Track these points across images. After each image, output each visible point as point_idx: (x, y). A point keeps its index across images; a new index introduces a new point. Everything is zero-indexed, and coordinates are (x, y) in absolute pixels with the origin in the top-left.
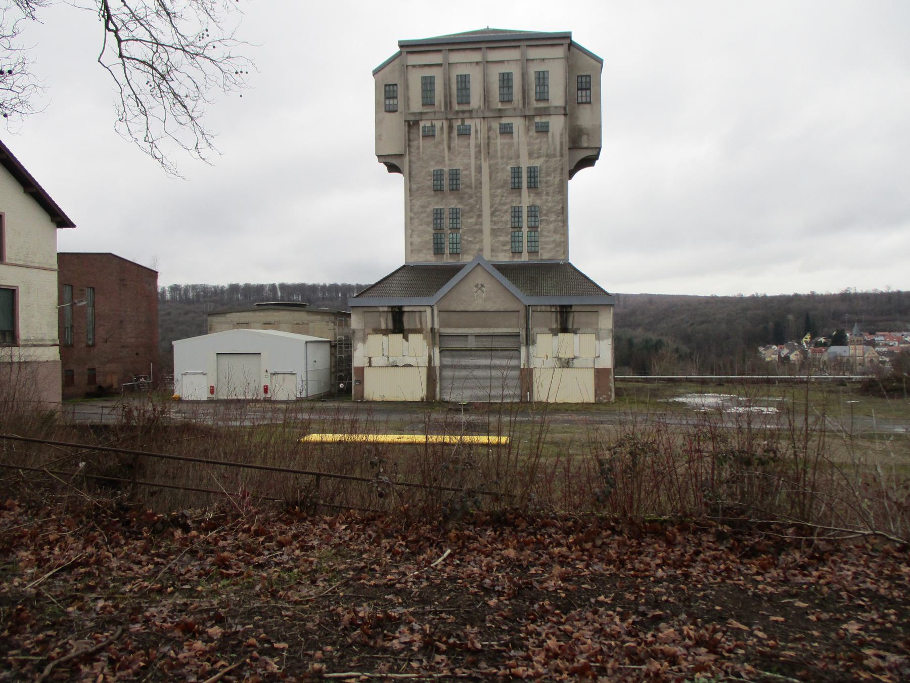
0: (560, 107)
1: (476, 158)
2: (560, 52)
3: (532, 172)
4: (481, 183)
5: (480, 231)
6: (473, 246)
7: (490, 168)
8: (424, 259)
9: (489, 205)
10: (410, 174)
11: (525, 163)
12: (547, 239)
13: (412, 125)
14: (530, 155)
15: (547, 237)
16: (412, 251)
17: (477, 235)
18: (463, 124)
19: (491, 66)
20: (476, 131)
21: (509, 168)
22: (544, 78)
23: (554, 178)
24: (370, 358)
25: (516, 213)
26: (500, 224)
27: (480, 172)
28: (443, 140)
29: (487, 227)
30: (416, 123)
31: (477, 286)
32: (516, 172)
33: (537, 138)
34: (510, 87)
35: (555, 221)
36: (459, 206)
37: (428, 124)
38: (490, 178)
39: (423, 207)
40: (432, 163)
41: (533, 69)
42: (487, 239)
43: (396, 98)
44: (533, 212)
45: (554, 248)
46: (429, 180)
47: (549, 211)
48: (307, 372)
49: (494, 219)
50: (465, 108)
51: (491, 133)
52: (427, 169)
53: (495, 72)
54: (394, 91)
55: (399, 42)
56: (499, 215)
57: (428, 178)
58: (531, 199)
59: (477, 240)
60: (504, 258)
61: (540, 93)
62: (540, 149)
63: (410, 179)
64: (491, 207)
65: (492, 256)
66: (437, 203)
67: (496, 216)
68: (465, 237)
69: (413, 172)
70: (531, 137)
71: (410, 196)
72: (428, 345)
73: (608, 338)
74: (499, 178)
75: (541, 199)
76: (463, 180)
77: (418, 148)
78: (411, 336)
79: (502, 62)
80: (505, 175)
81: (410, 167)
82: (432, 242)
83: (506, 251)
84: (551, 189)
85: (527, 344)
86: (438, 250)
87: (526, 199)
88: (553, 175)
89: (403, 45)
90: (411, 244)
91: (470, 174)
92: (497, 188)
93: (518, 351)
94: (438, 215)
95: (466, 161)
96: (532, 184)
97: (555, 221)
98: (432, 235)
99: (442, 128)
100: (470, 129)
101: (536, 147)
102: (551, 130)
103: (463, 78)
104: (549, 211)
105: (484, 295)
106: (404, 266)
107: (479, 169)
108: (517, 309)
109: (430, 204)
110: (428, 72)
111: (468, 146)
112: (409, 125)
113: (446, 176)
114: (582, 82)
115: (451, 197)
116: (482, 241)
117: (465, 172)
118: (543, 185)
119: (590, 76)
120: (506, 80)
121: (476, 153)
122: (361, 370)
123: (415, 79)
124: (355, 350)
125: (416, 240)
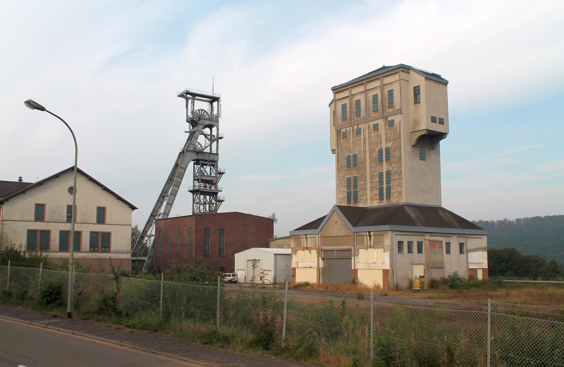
0: (399, 109)
1: (363, 146)
3: (387, 150)
4: (366, 161)
5: (366, 189)
7: (369, 151)
11: (384, 146)
14: (387, 141)
15: (395, 189)
21: (377, 150)
24: (298, 263)
25: (381, 175)
26: (374, 184)
28: (350, 138)
29: (368, 186)
31: (334, 222)
35: (398, 179)
36: (357, 175)
37: (344, 130)
39: (343, 177)
44: (388, 173)
45: (397, 196)
48: (276, 270)
50: (359, 118)
52: (344, 156)
53: (371, 94)
55: (332, 88)
56: (374, 178)
57: (345, 161)
59: (365, 194)
64: (370, 174)
65: (371, 203)
66: (348, 174)
67: (372, 179)
68: (360, 193)
69: (339, 158)
71: (338, 172)
73: (388, 251)
74: (373, 157)
75: (392, 166)
76: (358, 159)
78: (312, 251)
80: (376, 155)
82: (346, 196)
83: (376, 199)
84: (396, 160)
85: (355, 255)
87: (385, 168)
90: (339, 198)
91: (361, 156)
92: (373, 162)
94: (349, 180)
97: (398, 179)
98: (346, 193)
99: (350, 131)
101: (389, 135)
105: (337, 227)
107: (365, 152)
110: (344, 102)
111: (360, 140)
113: (352, 159)
115: (354, 170)
117: (359, 155)
121: (363, 143)
124: (292, 258)
125: (341, 196)
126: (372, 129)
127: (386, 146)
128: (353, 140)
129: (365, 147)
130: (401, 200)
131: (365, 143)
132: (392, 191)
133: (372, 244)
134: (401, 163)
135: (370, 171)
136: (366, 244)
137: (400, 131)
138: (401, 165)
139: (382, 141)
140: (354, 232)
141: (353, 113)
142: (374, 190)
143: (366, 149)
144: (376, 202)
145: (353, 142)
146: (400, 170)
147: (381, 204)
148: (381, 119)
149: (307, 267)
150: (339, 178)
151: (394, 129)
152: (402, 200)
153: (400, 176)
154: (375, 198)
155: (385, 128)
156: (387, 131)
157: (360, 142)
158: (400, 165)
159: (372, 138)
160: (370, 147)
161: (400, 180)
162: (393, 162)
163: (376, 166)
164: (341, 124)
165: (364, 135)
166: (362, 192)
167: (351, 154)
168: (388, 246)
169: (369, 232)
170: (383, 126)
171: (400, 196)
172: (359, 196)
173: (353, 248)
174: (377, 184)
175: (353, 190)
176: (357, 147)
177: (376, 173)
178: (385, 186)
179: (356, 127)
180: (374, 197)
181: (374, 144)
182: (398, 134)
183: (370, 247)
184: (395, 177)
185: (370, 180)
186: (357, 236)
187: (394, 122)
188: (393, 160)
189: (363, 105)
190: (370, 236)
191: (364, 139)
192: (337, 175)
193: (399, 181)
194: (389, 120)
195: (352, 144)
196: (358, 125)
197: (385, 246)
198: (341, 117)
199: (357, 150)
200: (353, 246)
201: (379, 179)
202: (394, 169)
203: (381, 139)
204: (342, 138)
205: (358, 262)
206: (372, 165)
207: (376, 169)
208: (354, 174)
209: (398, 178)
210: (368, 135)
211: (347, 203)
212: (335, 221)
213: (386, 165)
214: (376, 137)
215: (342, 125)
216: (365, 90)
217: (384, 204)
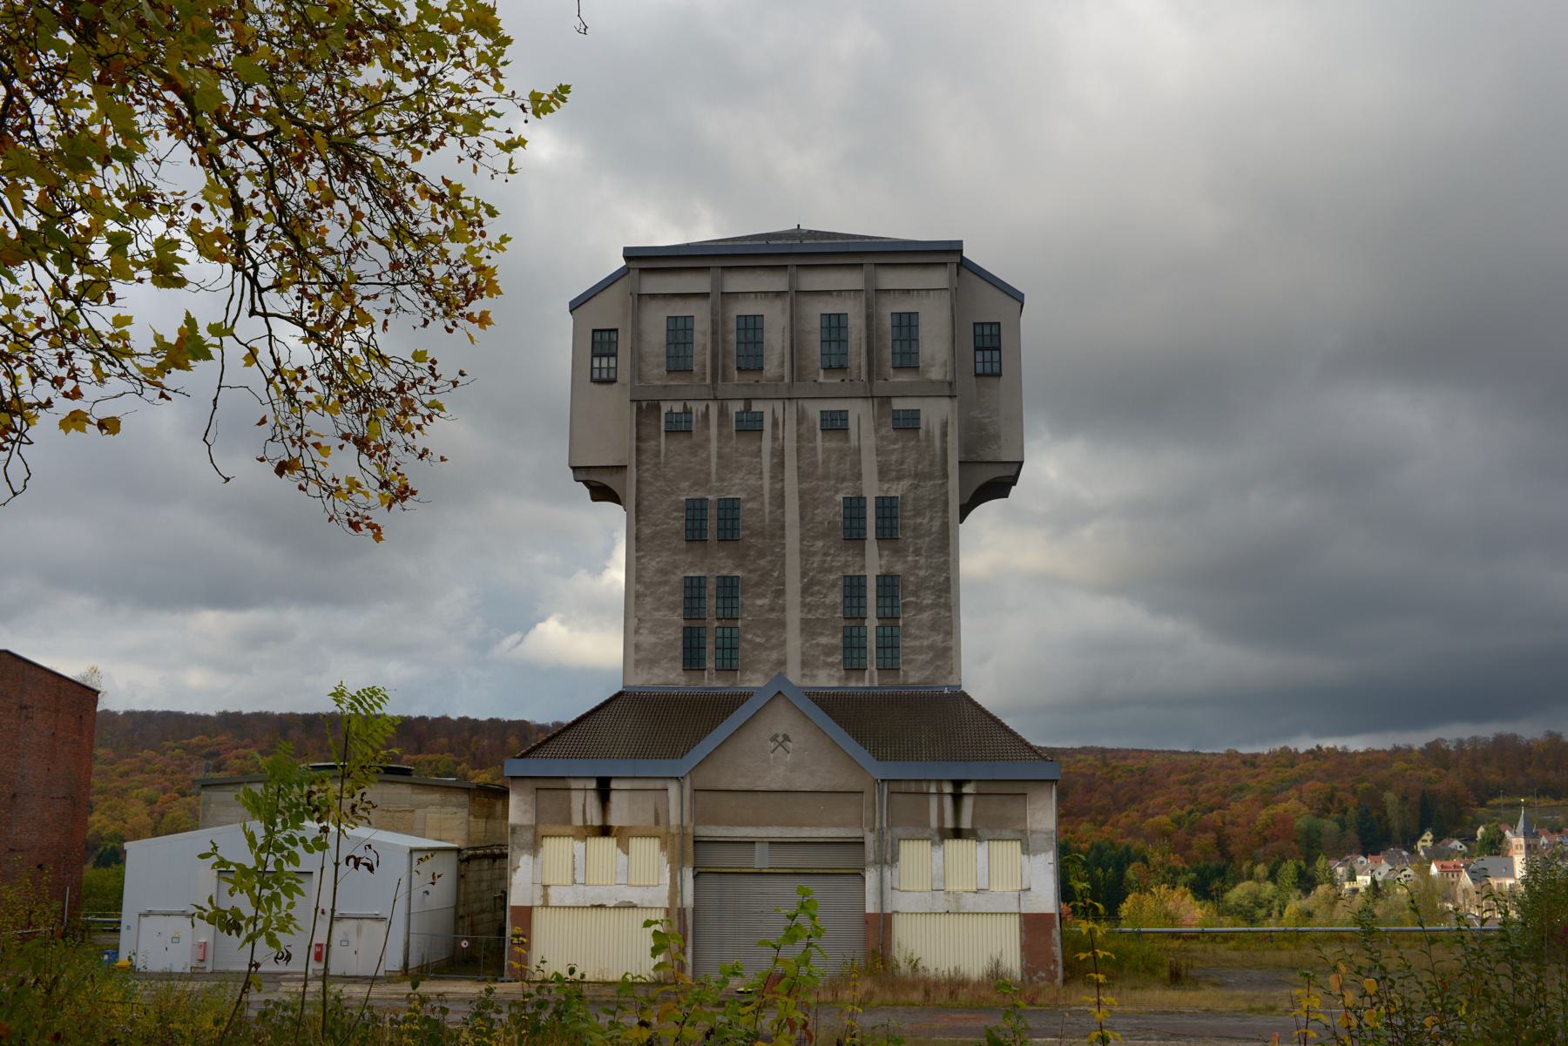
0: (942, 382)
1: (772, 478)
2: (938, 278)
3: (887, 507)
4: (783, 528)
5: (781, 625)
6: (764, 655)
7: (801, 498)
8: (662, 680)
9: (798, 571)
10: (638, 505)
11: (872, 489)
12: (917, 643)
13: (646, 410)
14: (883, 473)
15: (916, 638)
16: (638, 663)
17: (772, 633)
18: (748, 409)
19: (804, 299)
20: (775, 424)
21: (839, 498)
22: (910, 326)
23: (931, 519)
24: (546, 887)
25: (854, 587)
26: (821, 611)
27: (782, 505)
28: (708, 440)
29: (794, 616)
30: (655, 407)
31: (774, 739)
32: (854, 506)
33: (895, 442)
34: (842, 341)
35: (933, 606)
36: (738, 573)
38: (802, 518)
40: (685, 485)
41: (889, 308)
42: (794, 642)
43: (615, 355)
44: (889, 585)
45: (930, 662)
46: (675, 519)
47: (921, 586)
48: (409, 914)
49: (808, 600)
51: (804, 427)
52: (673, 498)
53: (815, 311)
54: (610, 342)
55: (625, 249)
57: (675, 514)
58: (883, 562)
59: (774, 641)
60: (827, 679)
61: (902, 354)
62: (902, 463)
63: (639, 516)
64: (803, 575)
65: (804, 676)
66: (692, 565)
67: (812, 595)
68: (749, 637)
69: (646, 503)
70: (883, 438)
71: (637, 551)
72: (671, 861)
73: (1045, 851)
74: (819, 519)
77: (657, 454)
79: (829, 292)
80: (832, 512)
81: (638, 489)
82: (680, 643)
83: (832, 665)
84: (924, 542)
86: (692, 659)
87: (874, 563)
88: (928, 514)
89: (631, 255)
90: (637, 647)
91: (762, 509)
92: (815, 538)
93: (860, 875)
94: (693, 590)
95: (752, 481)
96: (887, 531)
97: (933, 606)
98: (680, 630)
99: (706, 415)
100: (762, 421)
101: (894, 458)
102: (923, 424)
103: (750, 323)
104: (921, 586)
106: (620, 694)
107: (779, 499)
108: (858, 789)
109: (676, 567)
110: (680, 309)
111: (758, 453)
112: (639, 409)
113: (712, 513)
114: (983, 335)
115: (722, 554)
116: (784, 642)
117: (749, 505)
118: (909, 534)
119: (999, 323)
120: (835, 326)
121: (773, 468)
122: (525, 914)
123: (656, 320)
124: (515, 870)
125: (647, 639)
126: (818, 426)
127: (880, 489)
128: (720, 448)
129: (783, 480)
130: (945, 677)
131: (779, 466)
132: (907, 645)
133: (966, 824)
134: (949, 555)
135: (802, 567)
136: (934, 823)
137: (944, 451)
138: (946, 562)
139: (863, 472)
140: (882, 780)
141: (724, 357)
142: (822, 634)
143: (783, 487)
144: (829, 675)
145: (720, 456)
146: (942, 579)
147: (853, 684)
148: (860, 401)
149: (601, 906)
150: (643, 573)
151: (918, 441)
152: (950, 679)
153: (940, 597)
154: (824, 661)
155: (876, 431)
156: (885, 443)
157: (758, 459)
158: (942, 560)
159: (816, 455)
160: (806, 485)
161: (942, 612)
162: (911, 549)
163: (832, 551)
164: (658, 383)
165: (775, 438)
166: (759, 632)
167: (710, 497)
168: (1046, 833)
169: (958, 784)
170: (868, 424)
171: (939, 663)
172: (744, 645)
173: (870, 839)
174: (835, 613)
175: (716, 624)
176: (740, 475)
177: (831, 577)
178: (872, 623)
179: (736, 407)
180: (822, 658)
181: (825, 477)
182: (938, 459)
183: (957, 833)
184: (918, 597)
185: (802, 597)
186: (891, 793)
187: (919, 419)
188: (910, 540)
189: (775, 338)
190: (957, 798)
191: (779, 454)
192: (634, 562)
193: (938, 613)
194: (895, 408)
195: (714, 460)
196: (748, 401)
197: (1033, 832)
198: (664, 359)
199: (741, 484)
200: (872, 830)
201: (845, 597)
202: (917, 571)
203: (858, 463)
204: (663, 434)
205: (893, 888)
206: (812, 546)
207: (832, 561)
208: (724, 568)
209: (932, 604)
210: (798, 442)
211: (680, 665)
212: (777, 736)
213: (880, 556)
214: (834, 456)
215: (666, 386)
216: (790, 287)
217: (867, 684)
